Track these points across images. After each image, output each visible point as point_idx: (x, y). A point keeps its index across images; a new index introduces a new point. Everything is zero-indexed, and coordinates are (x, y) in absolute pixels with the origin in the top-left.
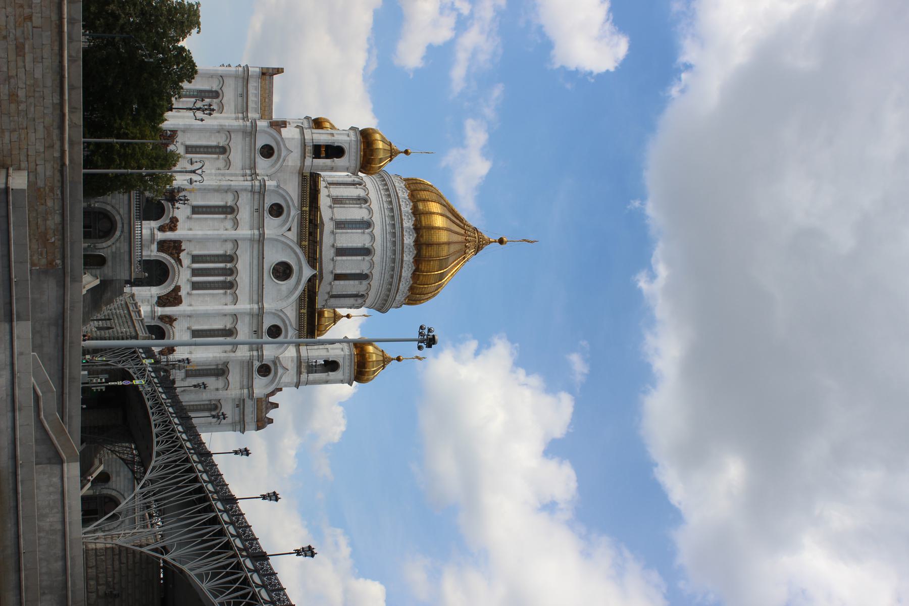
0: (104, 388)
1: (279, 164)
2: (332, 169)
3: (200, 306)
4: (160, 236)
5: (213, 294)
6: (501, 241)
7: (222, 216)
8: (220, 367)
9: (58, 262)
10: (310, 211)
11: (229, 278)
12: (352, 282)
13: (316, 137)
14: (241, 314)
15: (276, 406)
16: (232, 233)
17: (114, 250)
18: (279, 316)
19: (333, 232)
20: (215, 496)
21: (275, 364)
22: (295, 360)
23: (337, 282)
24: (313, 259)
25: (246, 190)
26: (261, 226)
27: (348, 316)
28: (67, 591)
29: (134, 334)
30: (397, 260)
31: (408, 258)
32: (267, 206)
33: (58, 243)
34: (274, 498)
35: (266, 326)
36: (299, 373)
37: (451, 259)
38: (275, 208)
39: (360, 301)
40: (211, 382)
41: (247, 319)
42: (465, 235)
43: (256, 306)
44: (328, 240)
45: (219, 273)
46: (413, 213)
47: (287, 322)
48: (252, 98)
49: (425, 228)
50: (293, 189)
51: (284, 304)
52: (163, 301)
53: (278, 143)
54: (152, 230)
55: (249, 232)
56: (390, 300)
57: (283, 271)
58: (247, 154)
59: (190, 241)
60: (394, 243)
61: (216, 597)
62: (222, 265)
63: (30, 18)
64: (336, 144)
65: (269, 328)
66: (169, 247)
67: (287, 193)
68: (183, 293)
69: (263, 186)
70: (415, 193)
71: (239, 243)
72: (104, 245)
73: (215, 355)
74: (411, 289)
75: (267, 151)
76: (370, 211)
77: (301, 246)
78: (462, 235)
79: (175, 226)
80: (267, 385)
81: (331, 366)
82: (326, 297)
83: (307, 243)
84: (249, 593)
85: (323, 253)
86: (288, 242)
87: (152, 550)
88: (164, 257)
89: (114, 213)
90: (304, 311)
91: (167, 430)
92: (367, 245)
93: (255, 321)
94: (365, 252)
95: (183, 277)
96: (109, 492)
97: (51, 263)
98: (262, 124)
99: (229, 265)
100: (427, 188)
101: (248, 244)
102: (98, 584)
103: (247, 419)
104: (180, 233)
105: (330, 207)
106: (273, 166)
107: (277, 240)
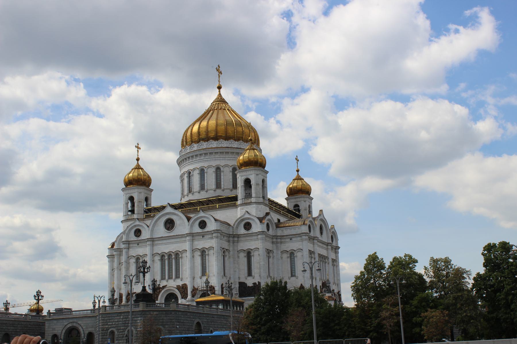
19: (193, 194)
22: (242, 207)
30: (205, 152)
35: (200, 230)
36: (250, 203)
41: (196, 243)
42: (214, 110)
47: (196, 217)
52: (185, 296)
60: (196, 156)
62: (166, 262)
71: (155, 252)
77: (154, 216)
80: (256, 223)
86: (152, 224)
93: (197, 238)
94: (202, 172)
95: (172, 284)
96: (63, 334)
99: (166, 257)
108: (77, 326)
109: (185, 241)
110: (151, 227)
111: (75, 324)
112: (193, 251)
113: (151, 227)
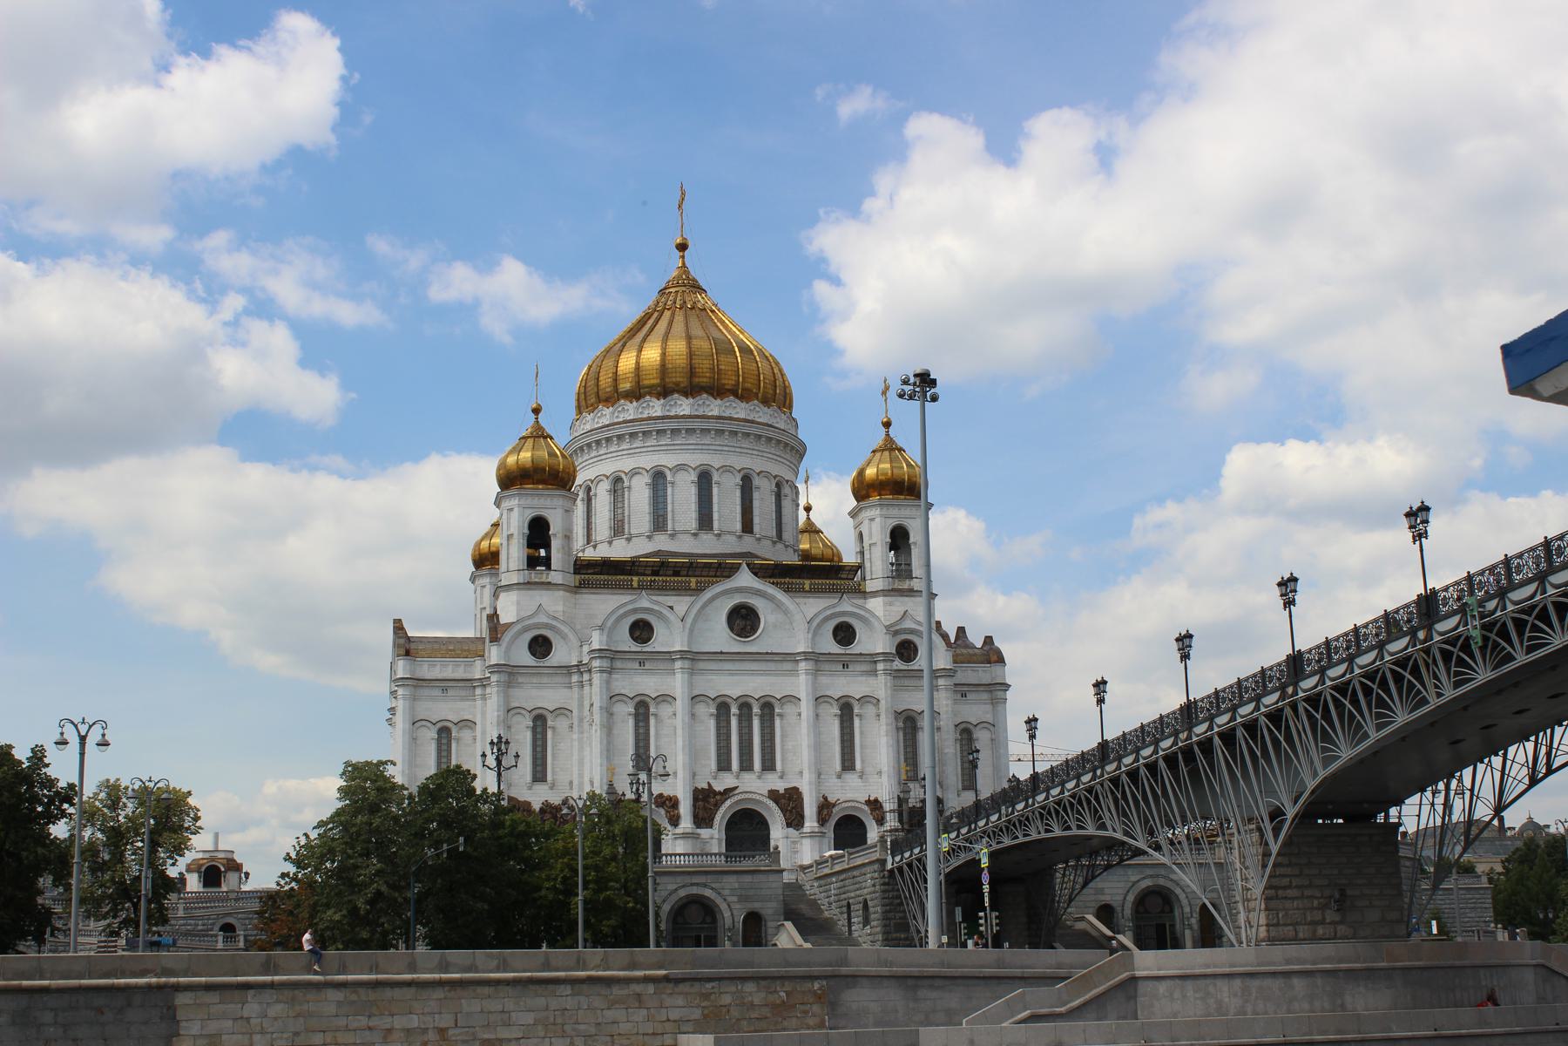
0: (995, 914)
1: (562, 627)
2: (568, 537)
3: (803, 755)
4: (686, 823)
5: (783, 736)
6: (682, 247)
7: (652, 721)
8: (901, 724)
9: (816, 986)
10: (637, 574)
11: (756, 710)
12: (756, 504)
13: (514, 565)
14: (815, 689)
15: (961, 630)
16: (681, 706)
17: (735, 899)
18: (819, 626)
19: (672, 536)
20: (1183, 736)
21: (896, 633)
23: (756, 529)
24: (721, 569)
25: (608, 682)
26: (669, 657)
27: (808, 509)
28: (1394, 969)
29: (876, 867)
31: (714, 407)
32: (635, 647)
33: (788, 986)
34: (1187, 641)
35: (836, 649)
36: (911, 592)
37: (716, 334)
38: (637, 633)
39: (786, 490)
40: (924, 739)
41: (824, 680)
42: (673, 309)
43: (803, 665)
44: (684, 542)
45: (746, 726)
46: (638, 399)
48: (449, 673)
49: (662, 379)
50: (606, 604)
51: (798, 617)
52: (794, 819)
53: (526, 629)
54: (677, 837)
55: (679, 676)
56: (783, 438)
57: (743, 620)
58: (545, 680)
59: (694, 775)
60: (690, 431)
61: (1366, 736)
62: (734, 722)
63: (442, 1031)
64: (526, 531)
65: (839, 642)
66: (705, 808)
67: (613, 612)
68: (781, 786)
69: (600, 653)
70: (602, 395)
71: (696, 692)
72: (727, 914)
73: (883, 732)
74: (766, 402)
75: (540, 646)
76: (635, 472)
78: (673, 315)
79: (670, 798)
81: (899, 539)
82: (780, 546)
83: (693, 580)
84: (1362, 684)
85: (708, 552)
87: (1276, 836)
88: (722, 815)
89: (674, 898)
90: (807, 583)
91: (1057, 812)
92: (694, 477)
93: (826, 666)
94: (704, 480)
95: (755, 786)
97: (819, 998)
98: (494, 655)
99: (734, 710)
100: (593, 375)
101: (698, 679)
102: (1322, 922)
103: (986, 679)
104: (679, 788)
105: (629, 540)
106: (564, 637)
107: (691, 631)
108: (1169, 885)
109: (794, 673)
110: (689, 620)
111: (1161, 882)
112: (819, 700)
113: (689, 620)
